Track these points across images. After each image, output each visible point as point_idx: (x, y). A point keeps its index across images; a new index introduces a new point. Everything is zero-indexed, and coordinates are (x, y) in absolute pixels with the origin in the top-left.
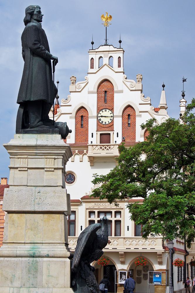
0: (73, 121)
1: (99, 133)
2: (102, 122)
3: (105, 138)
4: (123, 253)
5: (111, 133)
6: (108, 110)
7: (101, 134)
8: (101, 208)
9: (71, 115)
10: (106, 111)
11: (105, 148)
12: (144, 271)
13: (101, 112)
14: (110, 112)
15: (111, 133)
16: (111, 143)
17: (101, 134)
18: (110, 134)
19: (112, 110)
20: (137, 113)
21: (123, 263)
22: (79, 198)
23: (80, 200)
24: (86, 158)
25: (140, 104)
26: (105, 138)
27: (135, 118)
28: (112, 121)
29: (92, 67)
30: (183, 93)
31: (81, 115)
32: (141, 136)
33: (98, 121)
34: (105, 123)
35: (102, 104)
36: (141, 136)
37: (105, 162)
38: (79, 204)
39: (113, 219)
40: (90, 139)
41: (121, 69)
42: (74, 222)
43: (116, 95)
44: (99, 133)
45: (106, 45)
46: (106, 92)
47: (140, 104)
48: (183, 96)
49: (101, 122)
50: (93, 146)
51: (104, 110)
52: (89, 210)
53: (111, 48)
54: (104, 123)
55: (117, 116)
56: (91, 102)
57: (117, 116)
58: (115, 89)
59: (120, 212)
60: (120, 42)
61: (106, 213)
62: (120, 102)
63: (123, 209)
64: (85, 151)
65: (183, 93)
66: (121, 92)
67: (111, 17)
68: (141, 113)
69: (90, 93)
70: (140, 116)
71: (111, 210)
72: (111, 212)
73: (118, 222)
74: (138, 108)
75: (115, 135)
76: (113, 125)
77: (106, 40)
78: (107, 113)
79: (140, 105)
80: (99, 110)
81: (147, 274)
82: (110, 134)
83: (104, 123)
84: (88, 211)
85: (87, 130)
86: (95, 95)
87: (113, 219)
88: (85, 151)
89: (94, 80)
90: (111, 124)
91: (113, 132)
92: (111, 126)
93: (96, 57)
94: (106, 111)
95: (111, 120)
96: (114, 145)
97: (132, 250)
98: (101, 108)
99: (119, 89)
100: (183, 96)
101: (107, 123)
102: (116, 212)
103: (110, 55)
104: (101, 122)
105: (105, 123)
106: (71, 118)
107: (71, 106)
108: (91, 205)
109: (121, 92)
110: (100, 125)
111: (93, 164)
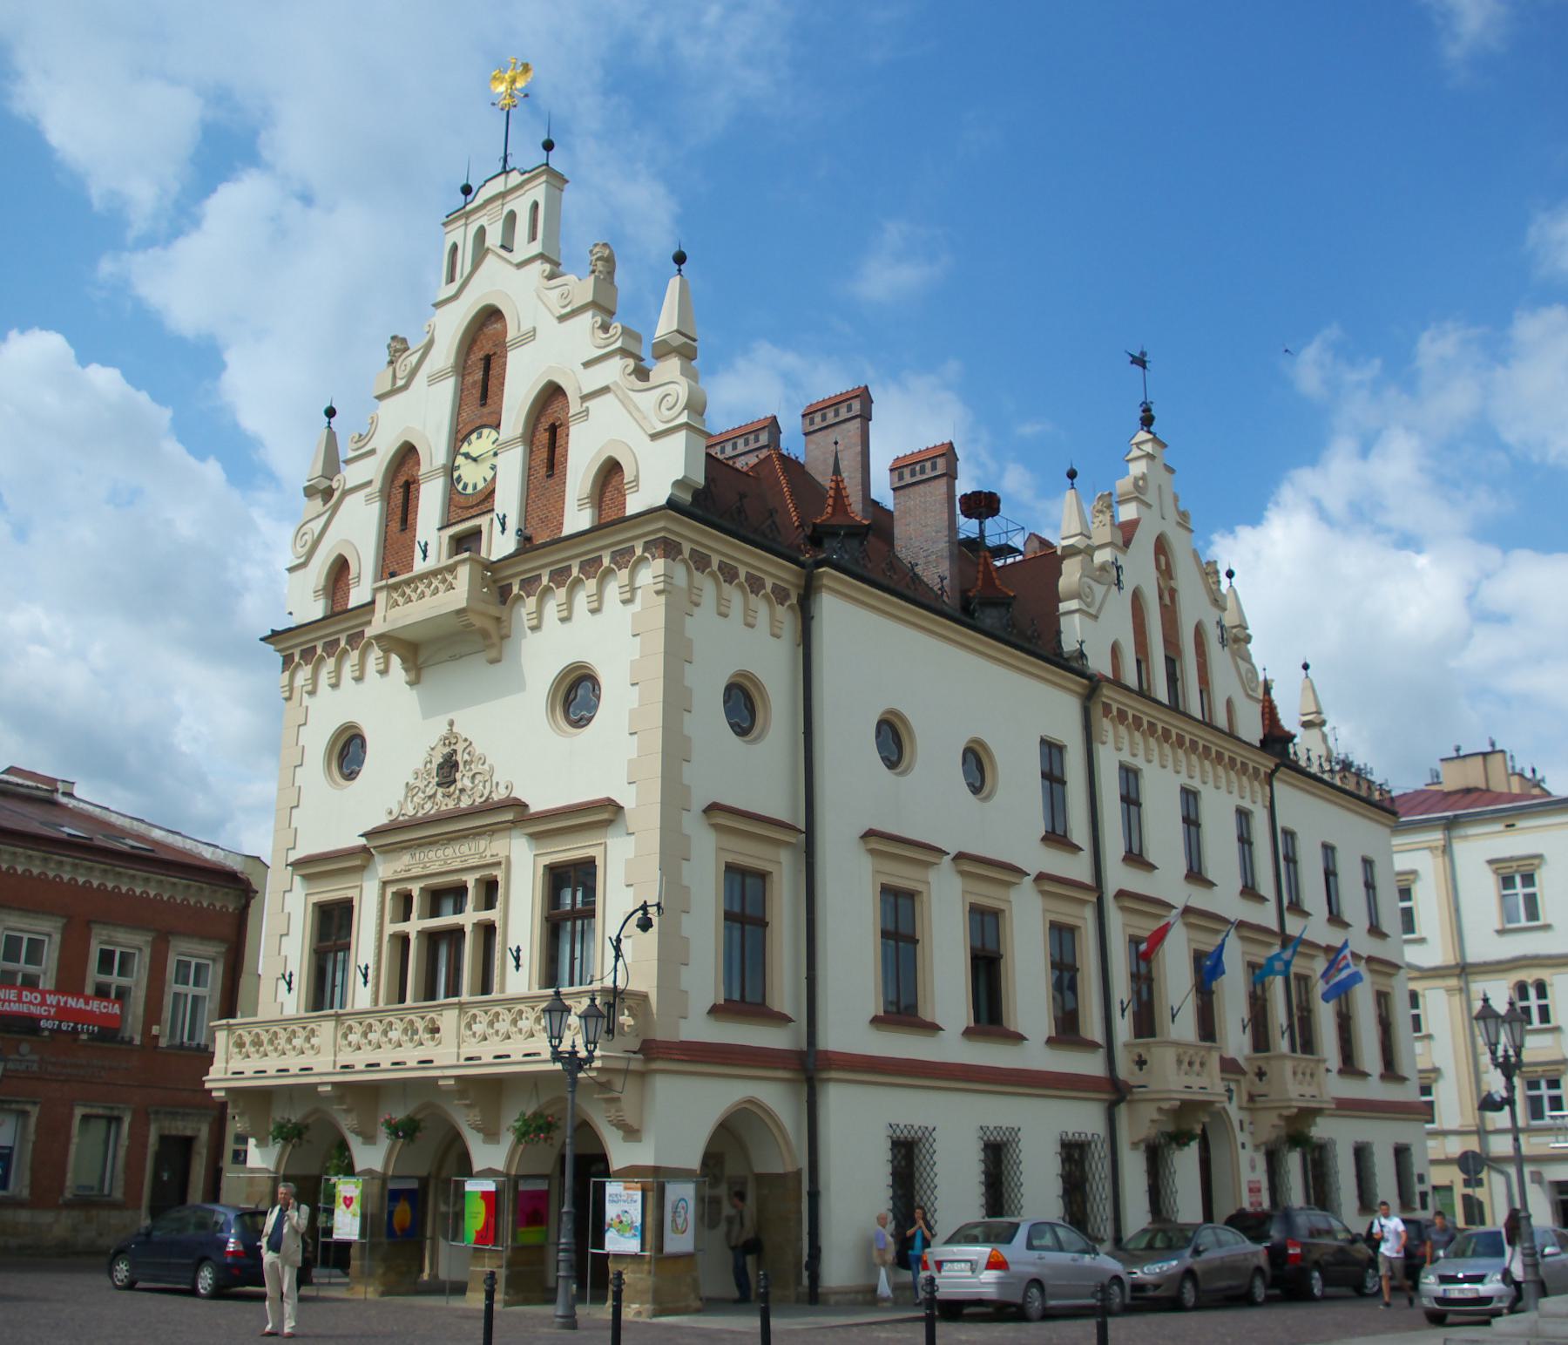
2: (465, 487)
4: (452, 1082)
5: (483, 521)
6: (486, 431)
8: (435, 868)
9: (368, 490)
14: (494, 434)
19: (497, 427)
20: (574, 406)
21: (491, 1135)
25: (587, 365)
29: (451, 279)
30: (1147, 410)
34: (475, 487)
35: (472, 412)
37: (453, 658)
38: (358, 862)
41: (536, 247)
47: (587, 365)
48: (1147, 421)
49: (460, 487)
53: (515, 178)
54: (470, 490)
55: (508, 444)
58: (511, 334)
63: (499, 863)
65: (1147, 410)
68: (589, 404)
69: (434, 379)
73: (488, 931)
74: (576, 382)
75: (497, 526)
77: (505, 161)
79: (592, 370)
80: (460, 436)
83: (470, 490)
84: (390, 890)
87: (469, 918)
89: (450, 326)
91: (487, 518)
93: (462, 235)
94: (479, 437)
99: (526, 327)
100: (1147, 421)
101: (481, 485)
104: (460, 487)
106: (368, 500)
107: (372, 452)
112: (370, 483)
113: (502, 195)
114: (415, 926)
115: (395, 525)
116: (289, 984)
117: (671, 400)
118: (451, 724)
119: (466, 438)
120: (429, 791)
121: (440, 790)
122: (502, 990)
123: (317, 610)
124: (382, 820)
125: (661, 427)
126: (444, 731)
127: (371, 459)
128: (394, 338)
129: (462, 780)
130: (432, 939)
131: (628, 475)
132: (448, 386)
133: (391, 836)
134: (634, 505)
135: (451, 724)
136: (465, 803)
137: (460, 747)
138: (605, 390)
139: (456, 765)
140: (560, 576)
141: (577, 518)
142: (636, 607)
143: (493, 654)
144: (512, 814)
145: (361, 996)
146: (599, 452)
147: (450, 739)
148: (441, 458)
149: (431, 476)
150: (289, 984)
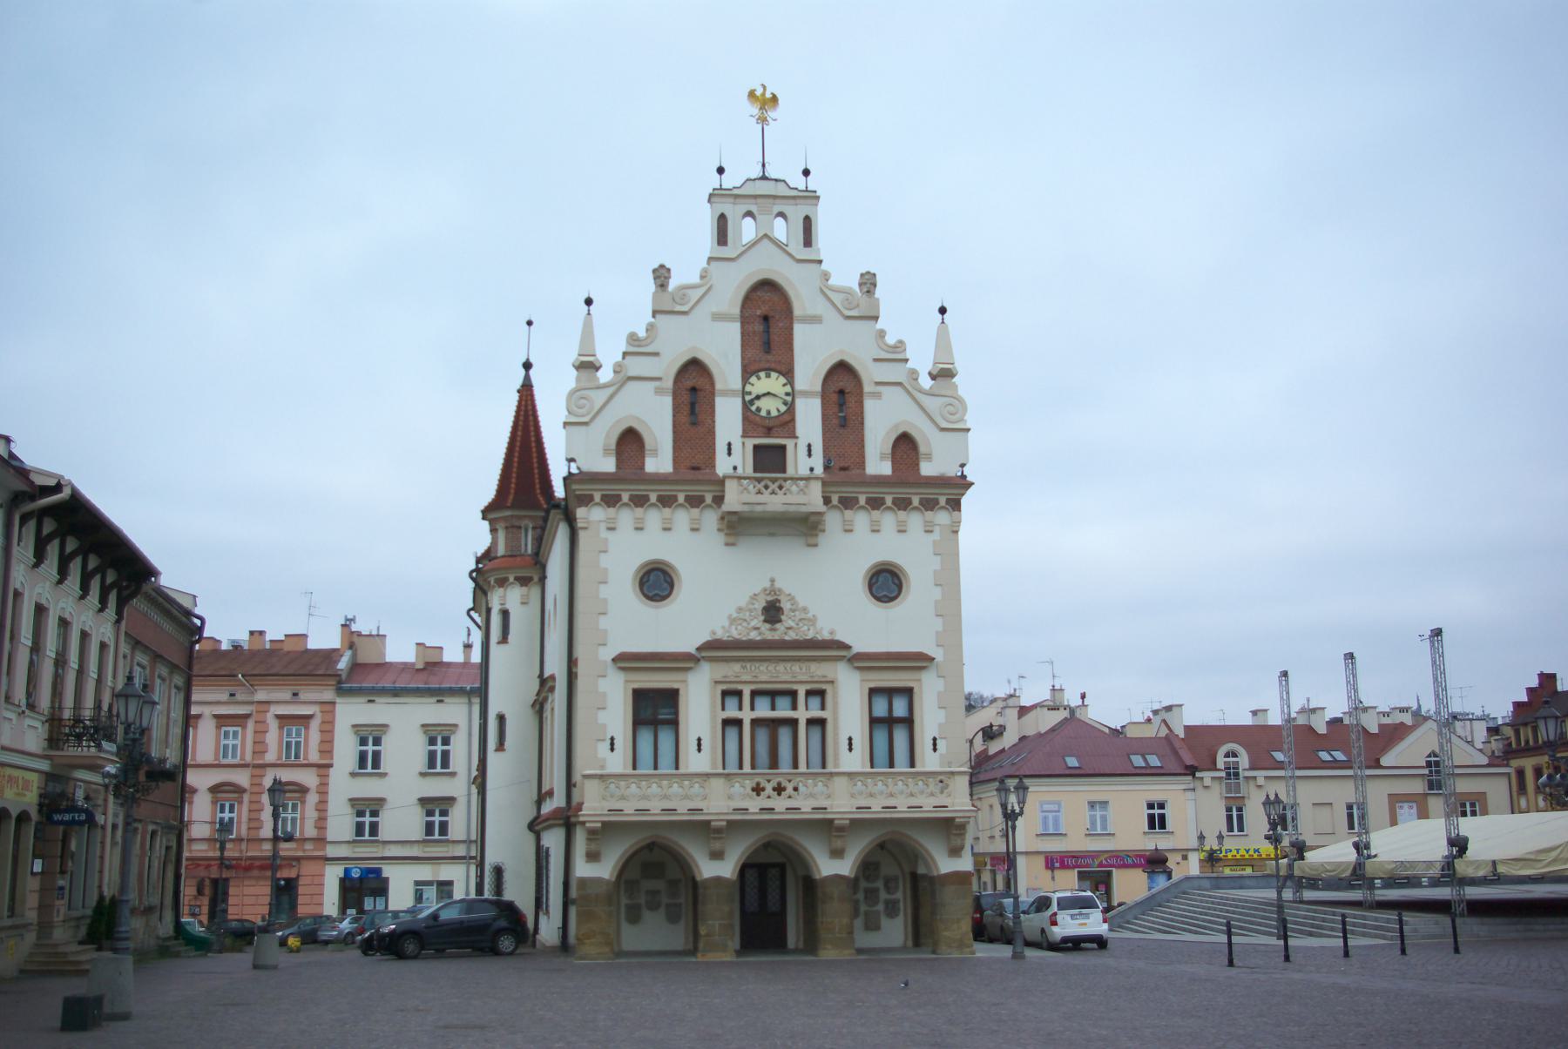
0: (668, 401)
1: (751, 443)
3: (770, 460)
5: (789, 443)
6: (774, 375)
7: (756, 447)
8: (763, 678)
9: (657, 384)
10: (768, 376)
11: (781, 487)
12: (867, 878)
13: (753, 379)
14: (782, 380)
15: (789, 443)
16: (790, 471)
17: (756, 447)
18: (783, 448)
19: (788, 373)
20: (868, 388)
22: (690, 646)
23: (693, 651)
24: (710, 519)
25: (876, 360)
26: (770, 460)
27: (860, 404)
28: (791, 408)
31: (690, 384)
32: (882, 458)
33: (746, 406)
36: (882, 458)
37: (772, 535)
39: (802, 715)
40: (723, 466)
42: (674, 723)
43: (799, 330)
44: (751, 443)
45: (764, 178)
46: (766, 318)
47: (876, 360)
50: (740, 478)
51: (762, 374)
52: (724, 687)
53: (781, 190)
54: (763, 413)
55: (806, 394)
56: (723, 350)
57: (806, 394)
58: (797, 312)
59: (821, 694)
60: (806, 173)
61: (773, 695)
62: (812, 353)
64: (709, 499)
66: (815, 320)
67: (774, 99)
69: (718, 317)
70: (877, 395)
71: (795, 687)
72: (793, 694)
75: (802, 450)
76: (793, 420)
78: (775, 383)
79: (879, 364)
80: (748, 372)
81: (877, 890)
82: (783, 448)
83: (763, 413)
85: (711, 433)
86: (738, 325)
88: (709, 499)
90: (787, 418)
92: (786, 423)
94: (768, 376)
95: (785, 403)
96: (807, 479)
97: (876, 807)
98: (753, 368)
99: (810, 312)
101: (774, 413)
102: (809, 693)
103: (777, 209)
105: (769, 412)
106: (659, 391)
107: (656, 354)
108: (732, 671)
109: (815, 320)
110: (752, 422)
111: (731, 540)
112: (659, 379)
113: (775, 197)
114: (747, 716)
115: (685, 418)
116: (612, 744)
117: (951, 409)
118: (773, 581)
119: (755, 372)
120: (754, 623)
121: (768, 626)
122: (836, 765)
123: (608, 465)
124: (708, 638)
125: (944, 425)
126: (768, 585)
127: (655, 359)
128: (662, 266)
129: (787, 621)
130: (755, 722)
131: (922, 449)
132: (734, 330)
133: (715, 649)
134: (927, 469)
135: (773, 581)
136: (791, 636)
137: (782, 598)
138: (899, 384)
139: (780, 610)
140: (875, 504)
141: (878, 464)
142: (936, 536)
143: (811, 540)
144: (833, 648)
145: (695, 762)
146: (896, 426)
147: (773, 590)
148: (735, 381)
149: (728, 393)
150: (612, 744)
